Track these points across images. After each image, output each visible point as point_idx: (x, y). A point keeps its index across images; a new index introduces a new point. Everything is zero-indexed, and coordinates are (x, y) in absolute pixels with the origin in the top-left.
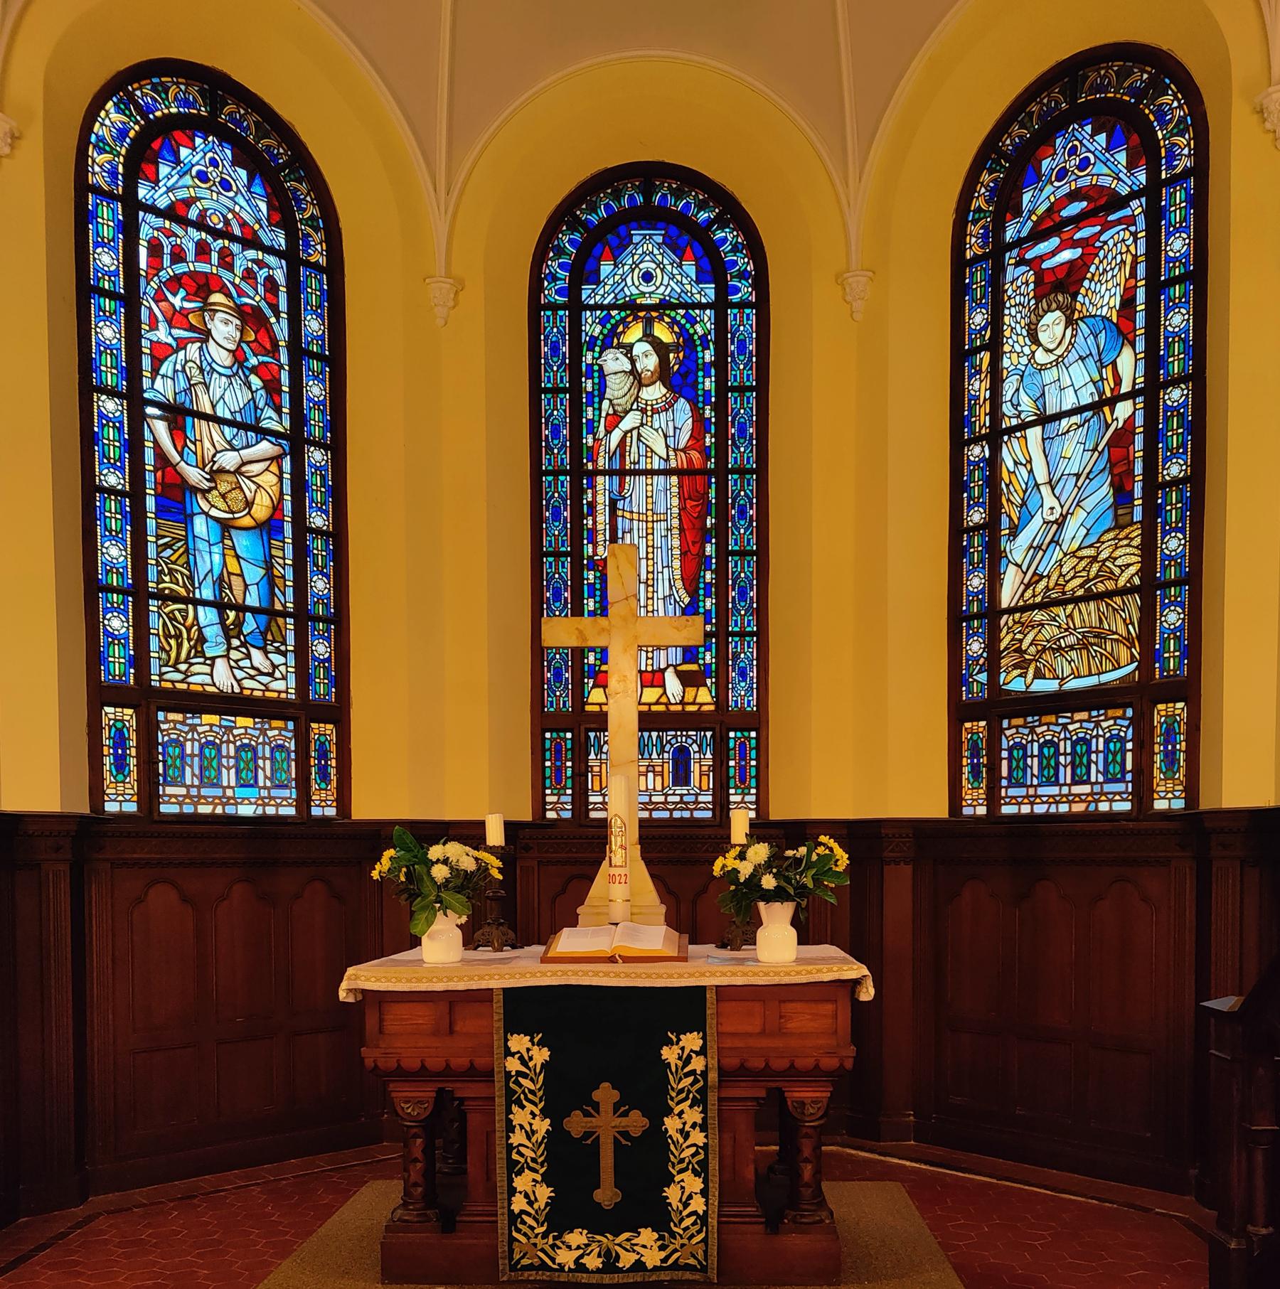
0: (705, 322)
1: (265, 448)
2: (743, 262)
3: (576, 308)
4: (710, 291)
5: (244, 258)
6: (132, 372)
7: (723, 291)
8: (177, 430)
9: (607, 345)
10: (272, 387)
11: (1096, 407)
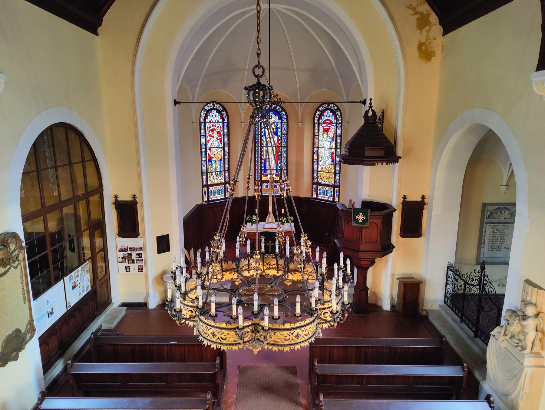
0: (279, 125)
2: (285, 117)
4: (280, 121)
7: (282, 121)
8: (210, 151)
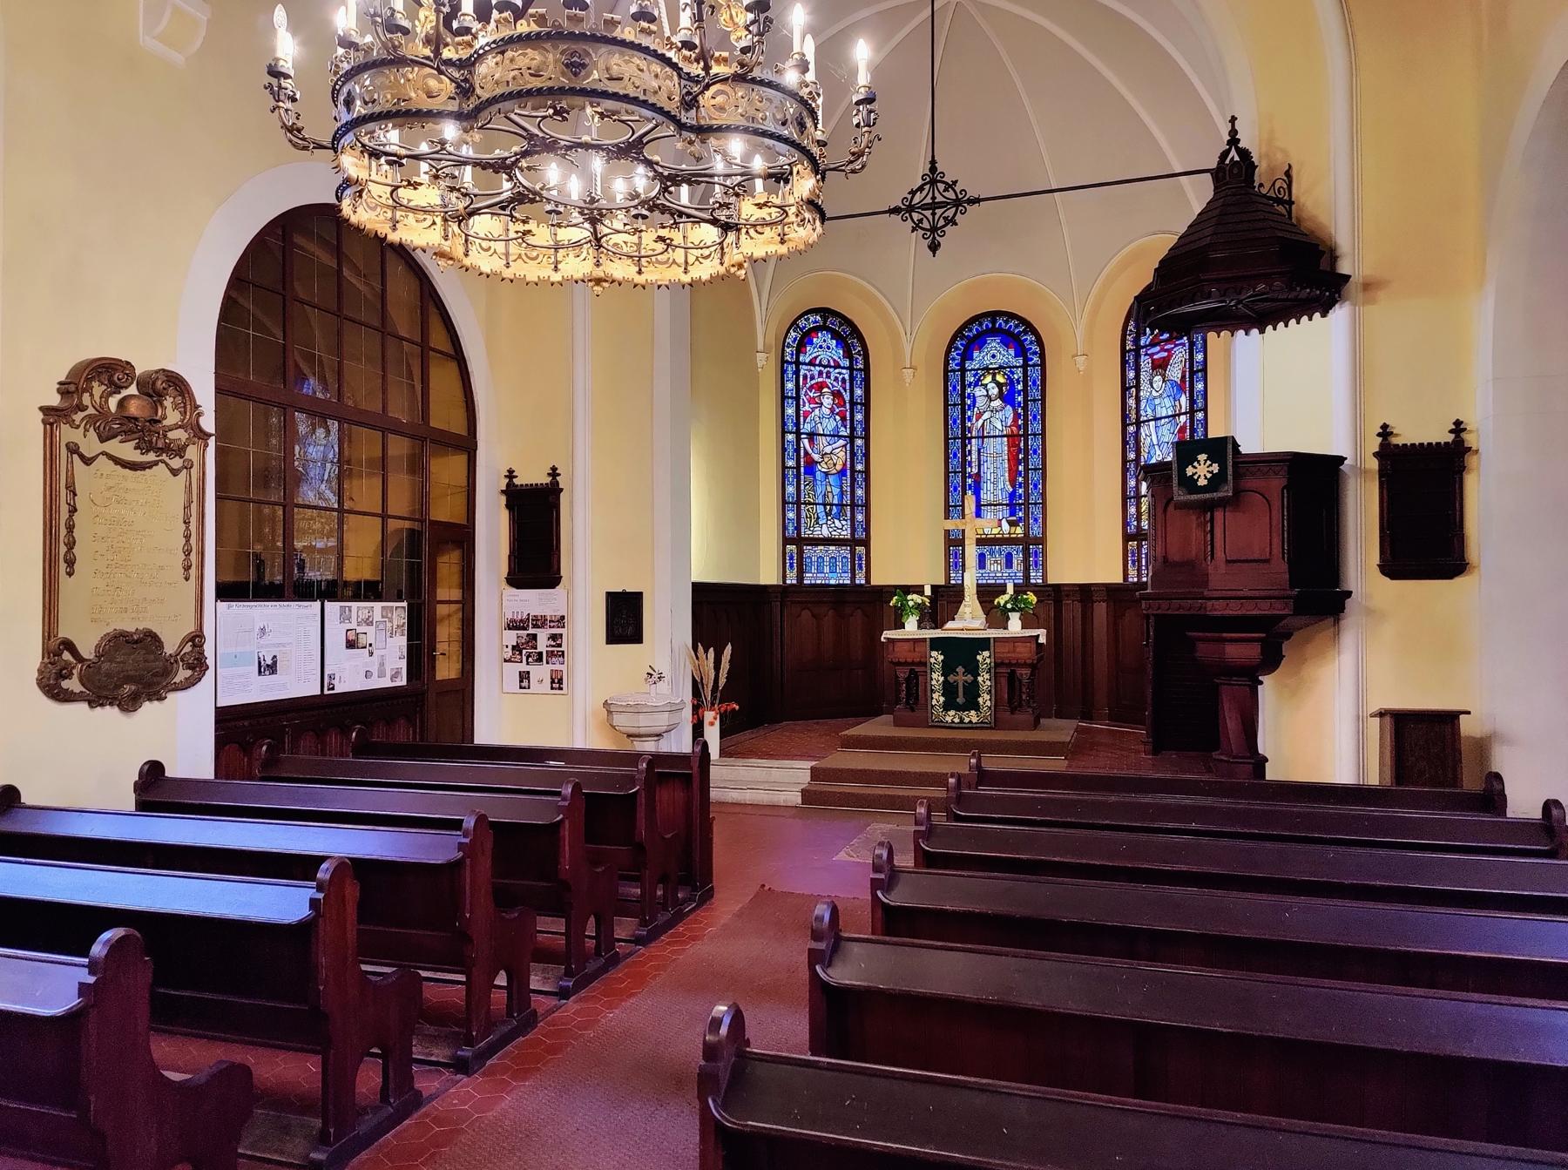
0: (1018, 374)
1: (841, 442)
2: (1035, 348)
3: (963, 371)
5: (834, 373)
6: (797, 424)
8: (811, 441)
9: (976, 385)
10: (843, 419)
11: (1173, 416)
